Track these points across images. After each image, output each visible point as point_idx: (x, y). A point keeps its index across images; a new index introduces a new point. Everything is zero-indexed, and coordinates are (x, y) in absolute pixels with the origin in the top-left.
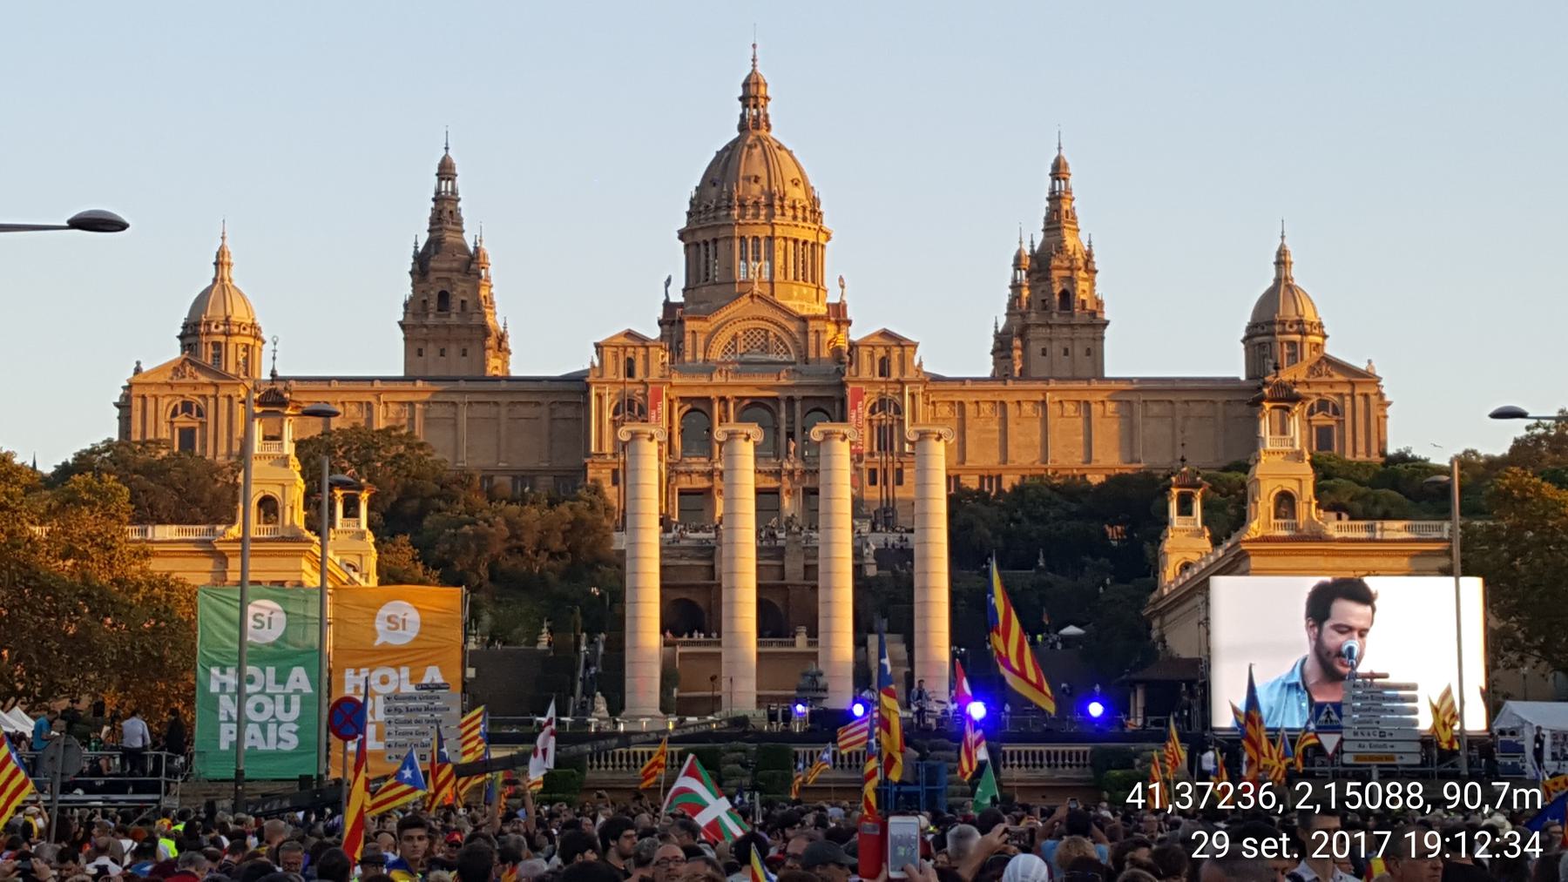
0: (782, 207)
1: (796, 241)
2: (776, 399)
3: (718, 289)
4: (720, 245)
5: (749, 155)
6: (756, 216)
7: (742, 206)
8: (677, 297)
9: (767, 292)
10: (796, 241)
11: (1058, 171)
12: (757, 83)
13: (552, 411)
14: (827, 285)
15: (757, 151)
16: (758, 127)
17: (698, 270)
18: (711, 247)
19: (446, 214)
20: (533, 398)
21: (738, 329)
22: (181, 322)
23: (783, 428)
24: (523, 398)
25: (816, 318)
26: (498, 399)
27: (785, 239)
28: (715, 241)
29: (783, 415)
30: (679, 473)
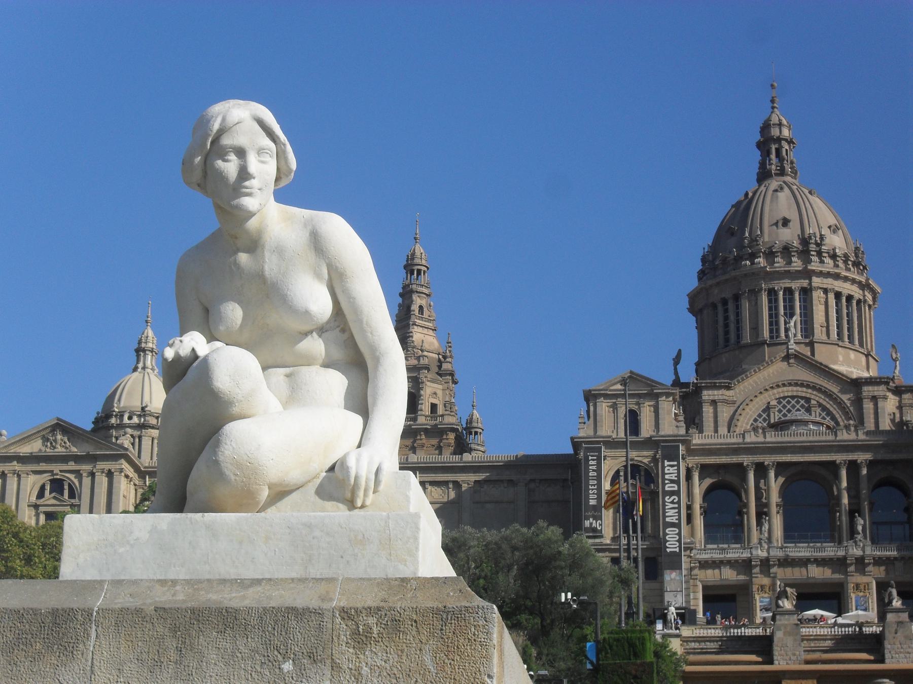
0: (819, 254)
1: (838, 295)
5: (774, 199)
6: (789, 263)
7: (770, 255)
8: (688, 374)
9: (807, 351)
10: (838, 295)
12: (780, 125)
15: (784, 196)
16: (782, 172)
18: (731, 306)
19: (415, 308)
21: (771, 397)
22: (93, 416)
25: (870, 381)
26: (460, 477)
27: (826, 291)
28: (737, 298)
30: (705, 565)
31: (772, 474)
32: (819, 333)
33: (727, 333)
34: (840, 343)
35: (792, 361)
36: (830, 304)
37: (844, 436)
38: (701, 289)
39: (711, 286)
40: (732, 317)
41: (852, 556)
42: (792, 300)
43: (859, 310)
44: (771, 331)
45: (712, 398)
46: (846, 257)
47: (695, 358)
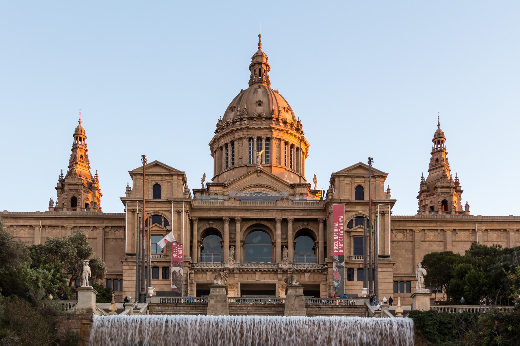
1: (286, 143)
2: (273, 220)
3: (233, 172)
4: (236, 143)
9: (266, 170)
10: (286, 143)
11: (439, 138)
13: (106, 233)
14: (306, 176)
17: (221, 166)
20: (92, 223)
23: (279, 241)
24: (84, 223)
27: (280, 140)
28: (232, 143)
29: (279, 232)
31: (238, 225)
32: (274, 162)
33: (227, 162)
34: (286, 168)
35: (259, 174)
36: (282, 147)
37: (281, 204)
38: (215, 139)
39: (220, 137)
40: (230, 153)
41: (281, 269)
42: (261, 144)
43: (297, 154)
44: (250, 160)
45: (215, 192)
46: (292, 125)
47: (212, 176)
